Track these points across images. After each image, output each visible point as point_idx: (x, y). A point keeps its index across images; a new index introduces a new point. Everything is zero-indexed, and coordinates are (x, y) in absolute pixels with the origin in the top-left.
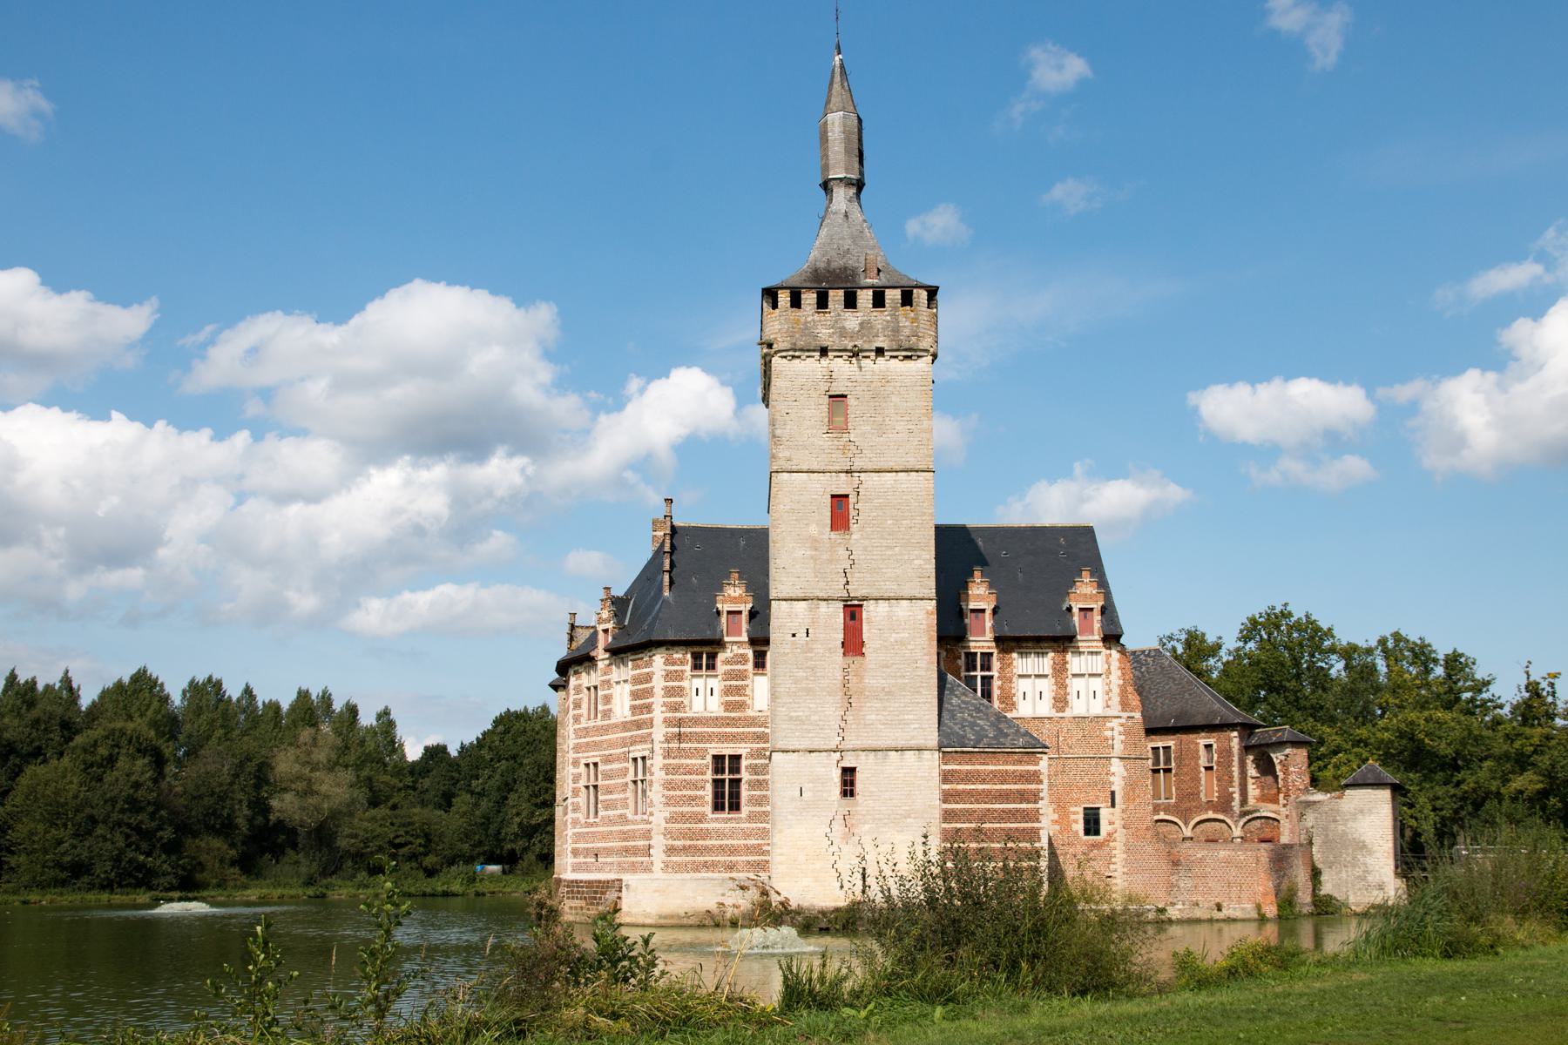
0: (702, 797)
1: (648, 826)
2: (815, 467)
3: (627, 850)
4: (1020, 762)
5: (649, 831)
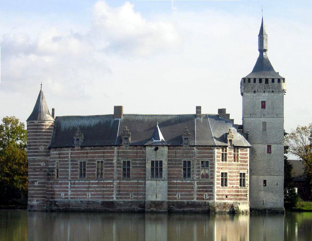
1: (246, 190)
3: (238, 195)
5: (247, 191)
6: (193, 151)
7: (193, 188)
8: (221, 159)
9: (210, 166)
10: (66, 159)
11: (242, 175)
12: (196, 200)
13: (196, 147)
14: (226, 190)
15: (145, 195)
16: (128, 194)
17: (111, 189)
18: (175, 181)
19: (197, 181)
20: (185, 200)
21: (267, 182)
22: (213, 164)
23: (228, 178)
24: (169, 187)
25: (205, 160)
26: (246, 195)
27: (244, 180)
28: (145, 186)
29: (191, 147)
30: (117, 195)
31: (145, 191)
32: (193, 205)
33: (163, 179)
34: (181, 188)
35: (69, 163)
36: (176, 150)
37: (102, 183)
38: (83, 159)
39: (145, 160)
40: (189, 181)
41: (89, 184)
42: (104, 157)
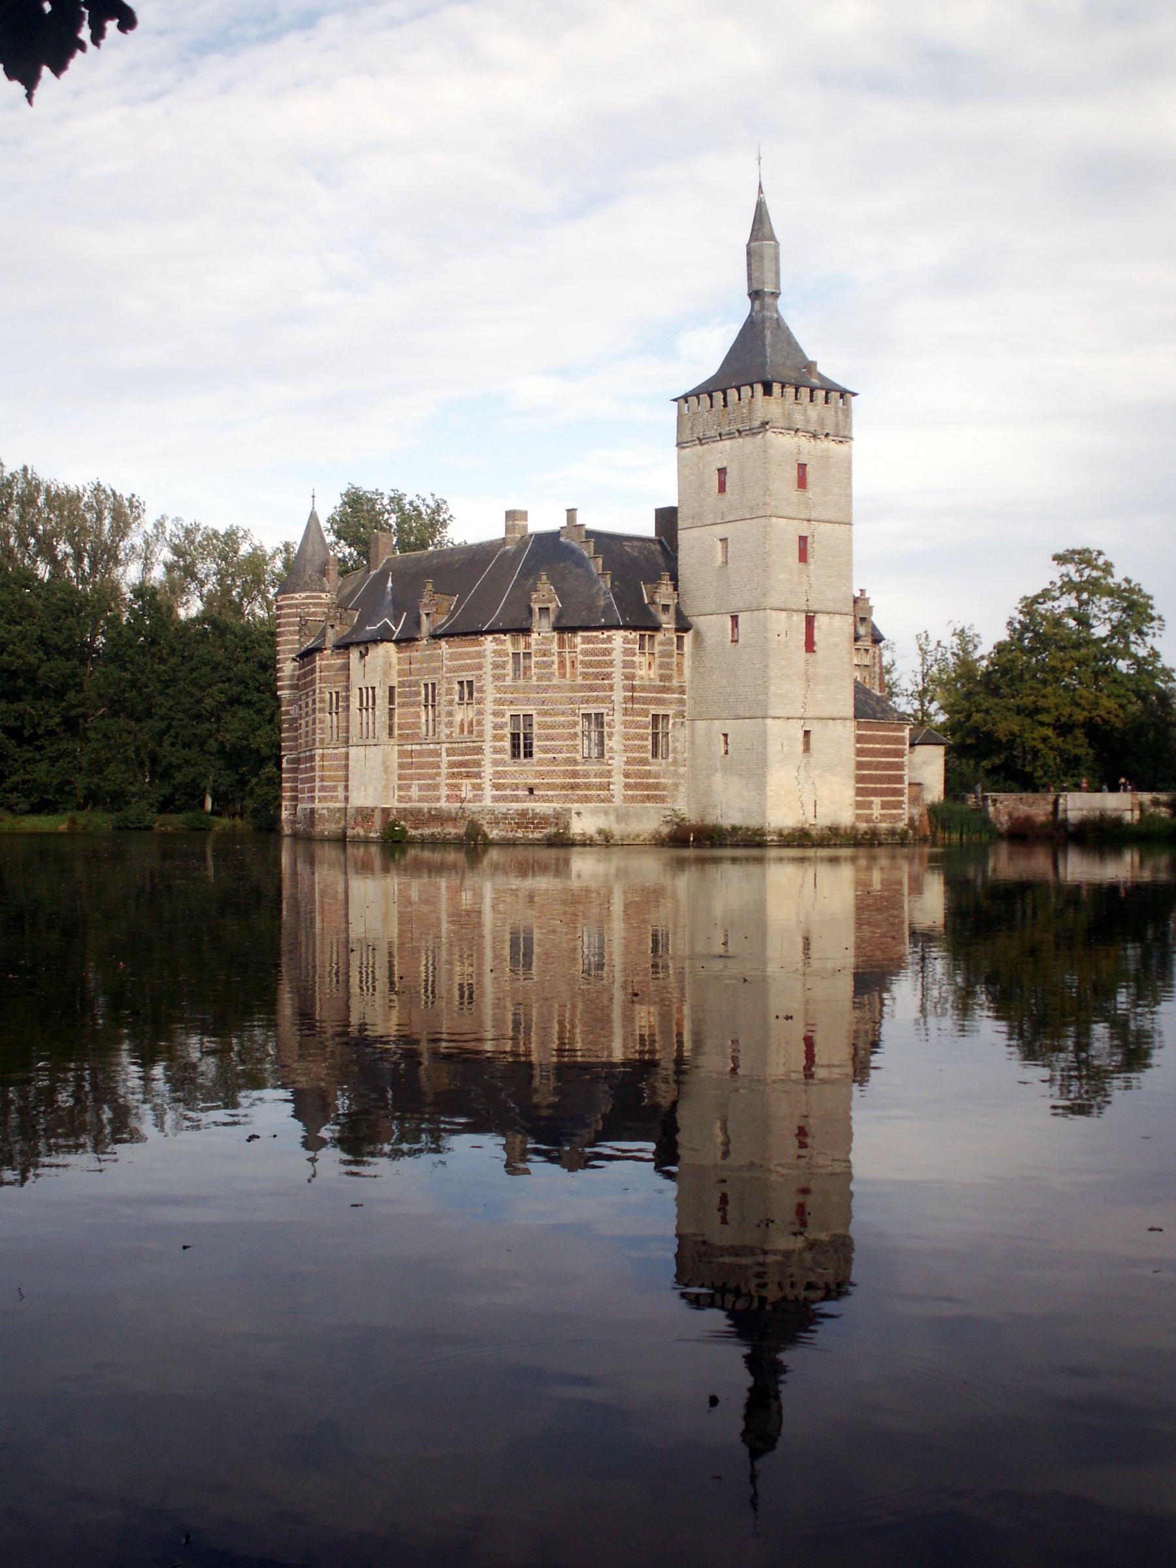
0: (646, 746)
2: (790, 515)
3: (573, 787)
4: (894, 730)
5: (609, 772)
14: (525, 772)
22: (481, 690)
23: (536, 729)
25: (466, 676)
32: (439, 817)
33: (375, 741)
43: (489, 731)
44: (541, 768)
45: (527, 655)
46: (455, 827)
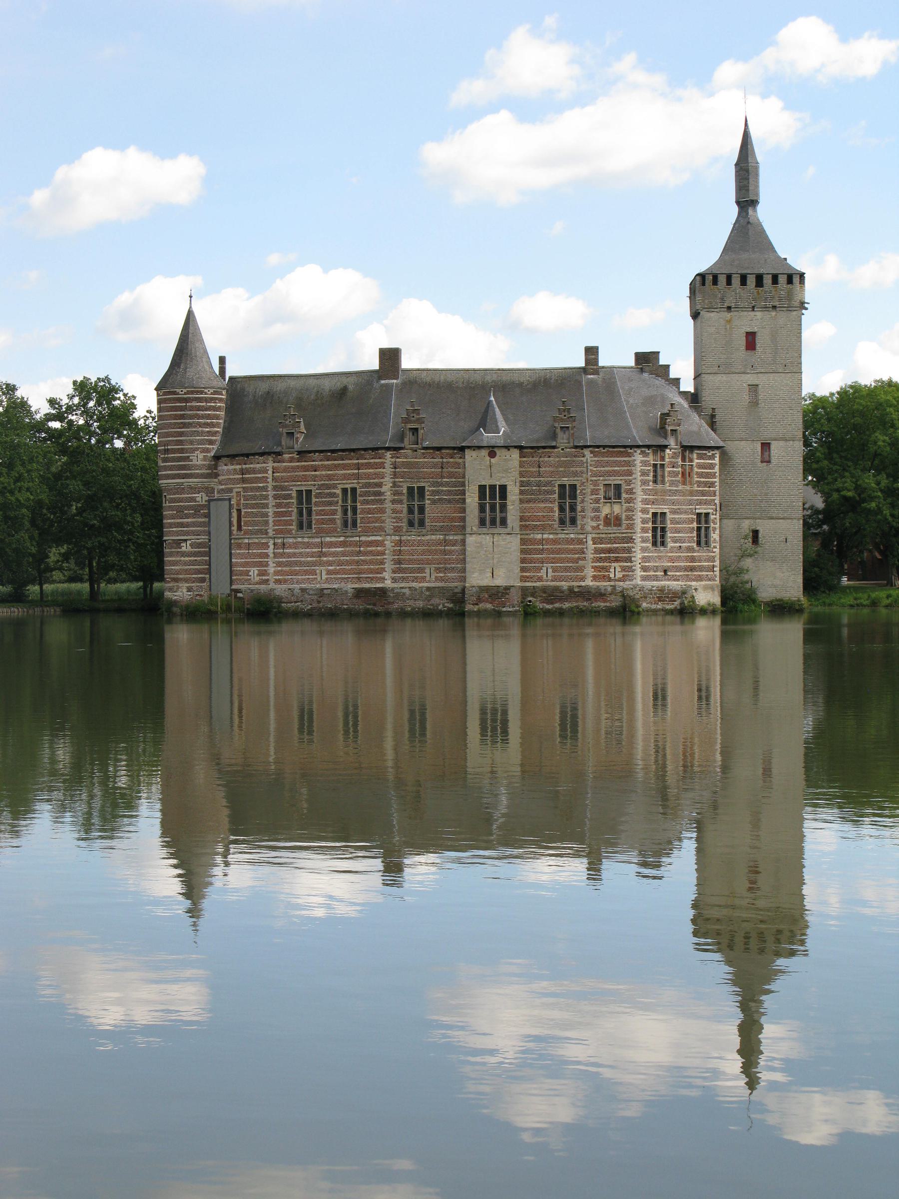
1: (713, 554)
3: (692, 569)
5: (714, 557)
6: (582, 459)
7: (584, 553)
8: (651, 478)
9: (624, 495)
10: (261, 485)
11: (701, 517)
12: (592, 581)
13: (591, 449)
14: (663, 557)
15: (464, 570)
16: (421, 570)
17: (379, 557)
18: (539, 536)
19: (594, 536)
20: (563, 583)
21: (760, 535)
22: (631, 492)
23: (669, 525)
24: (523, 551)
26: (712, 569)
27: (707, 529)
28: (462, 547)
29: (578, 450)
30: (394, 572)
31: (464, 561)
32: (586, 594)
34: (553, 552)
35: (269, 493)
36: (541, 457)
37: (356, 544)
38: (303, 483)
39: (463, 485)
40: (572, 536)
41: (322, 545)
42: (358, 476)
43: (639, 525)
44: (672, 554)
45: (662, 466)
46: (605, 601)
